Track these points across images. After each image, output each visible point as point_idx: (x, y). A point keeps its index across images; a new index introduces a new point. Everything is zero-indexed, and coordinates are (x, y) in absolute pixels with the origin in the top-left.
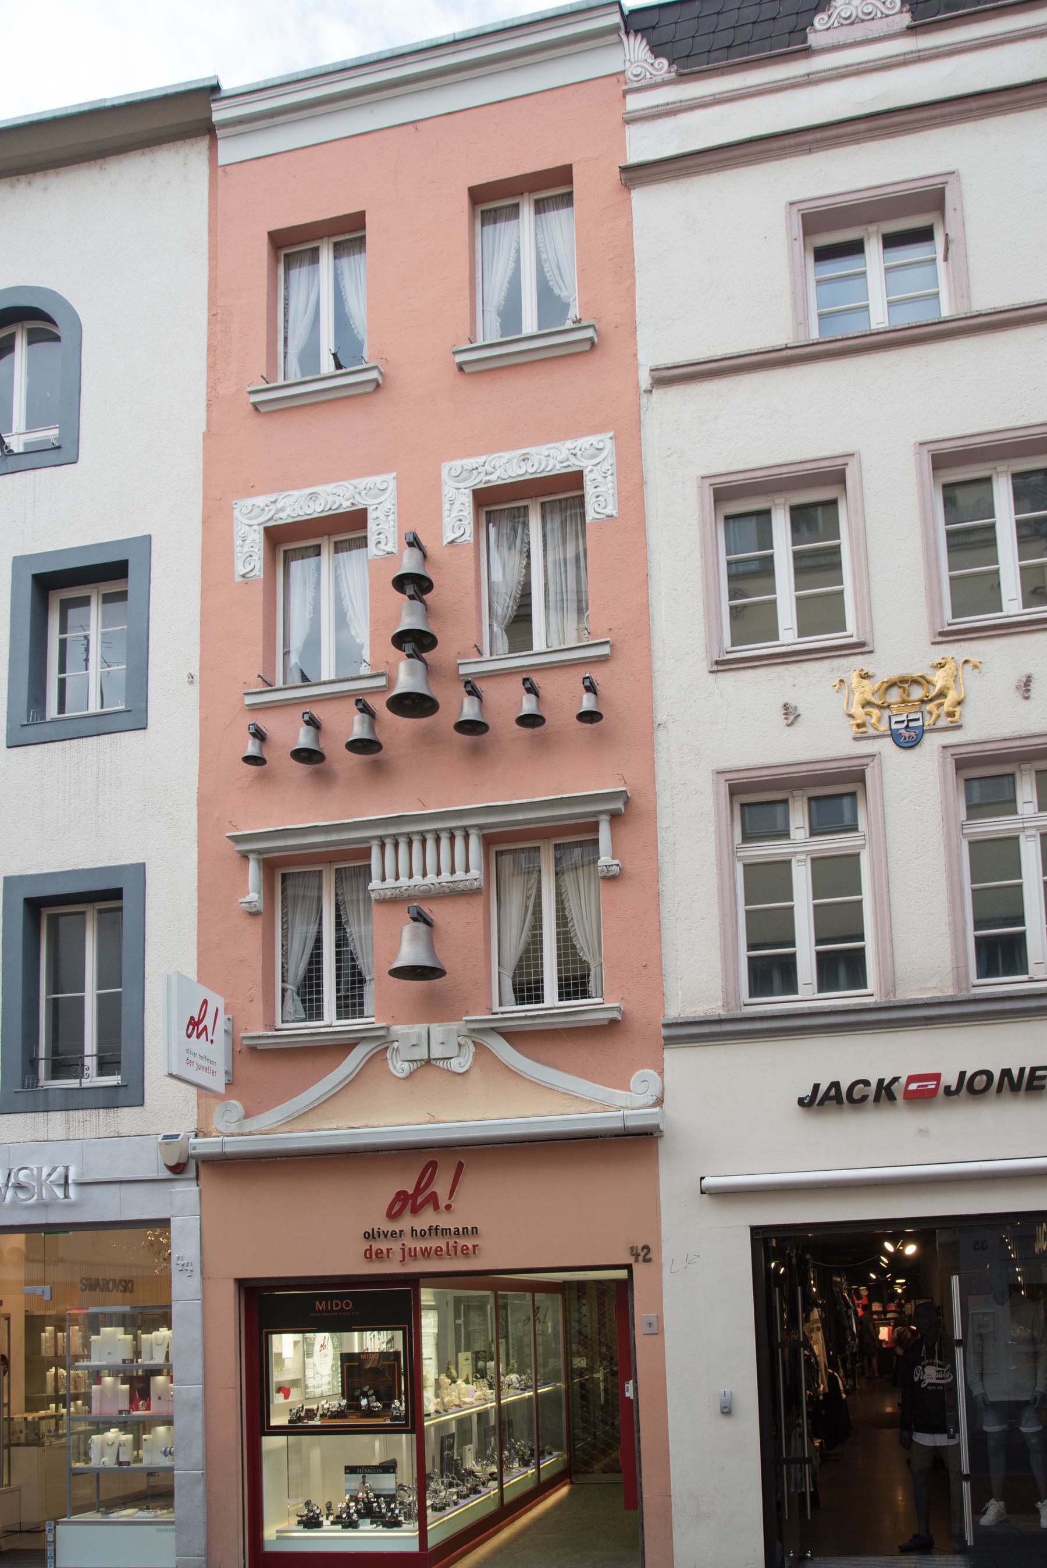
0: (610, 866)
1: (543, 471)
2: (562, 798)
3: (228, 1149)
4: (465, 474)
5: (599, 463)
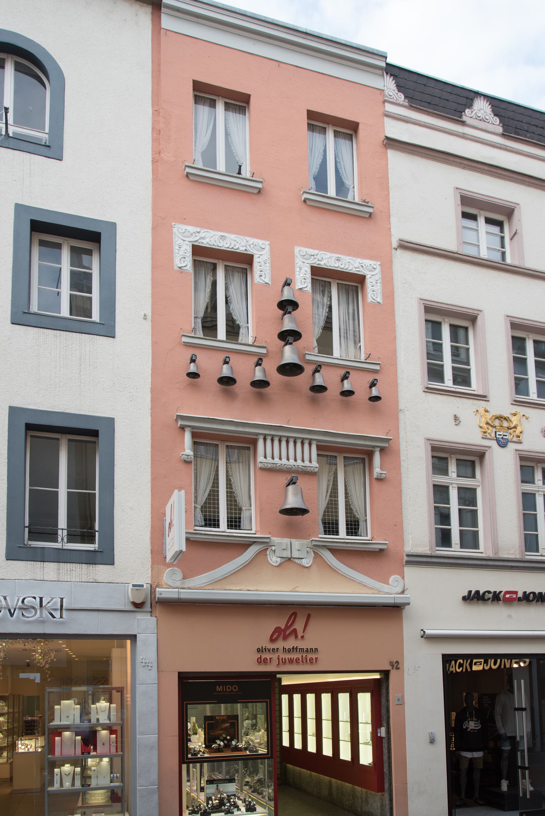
0: (382, 474)
1: (347, 269)
2: (363, 436)
3: (182, 596)
4: (307, 256)
5: (374, 275)
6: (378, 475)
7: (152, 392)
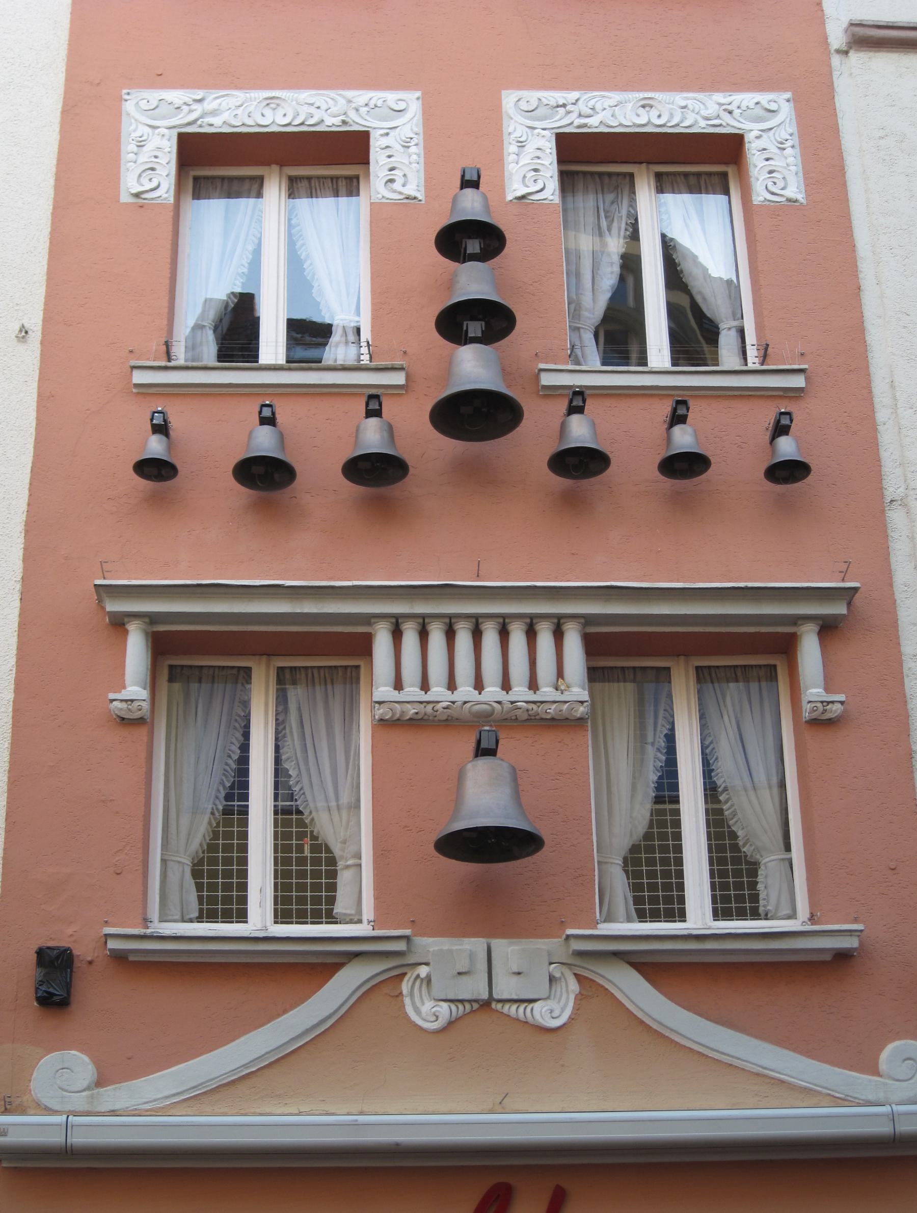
0: (828, 703)
1: (677, 125)
2: (746, 588)
3: (78, 1139)
4: (541, 111)
5: (771, 129)
6: (813, 710)
7: (27, 532)
